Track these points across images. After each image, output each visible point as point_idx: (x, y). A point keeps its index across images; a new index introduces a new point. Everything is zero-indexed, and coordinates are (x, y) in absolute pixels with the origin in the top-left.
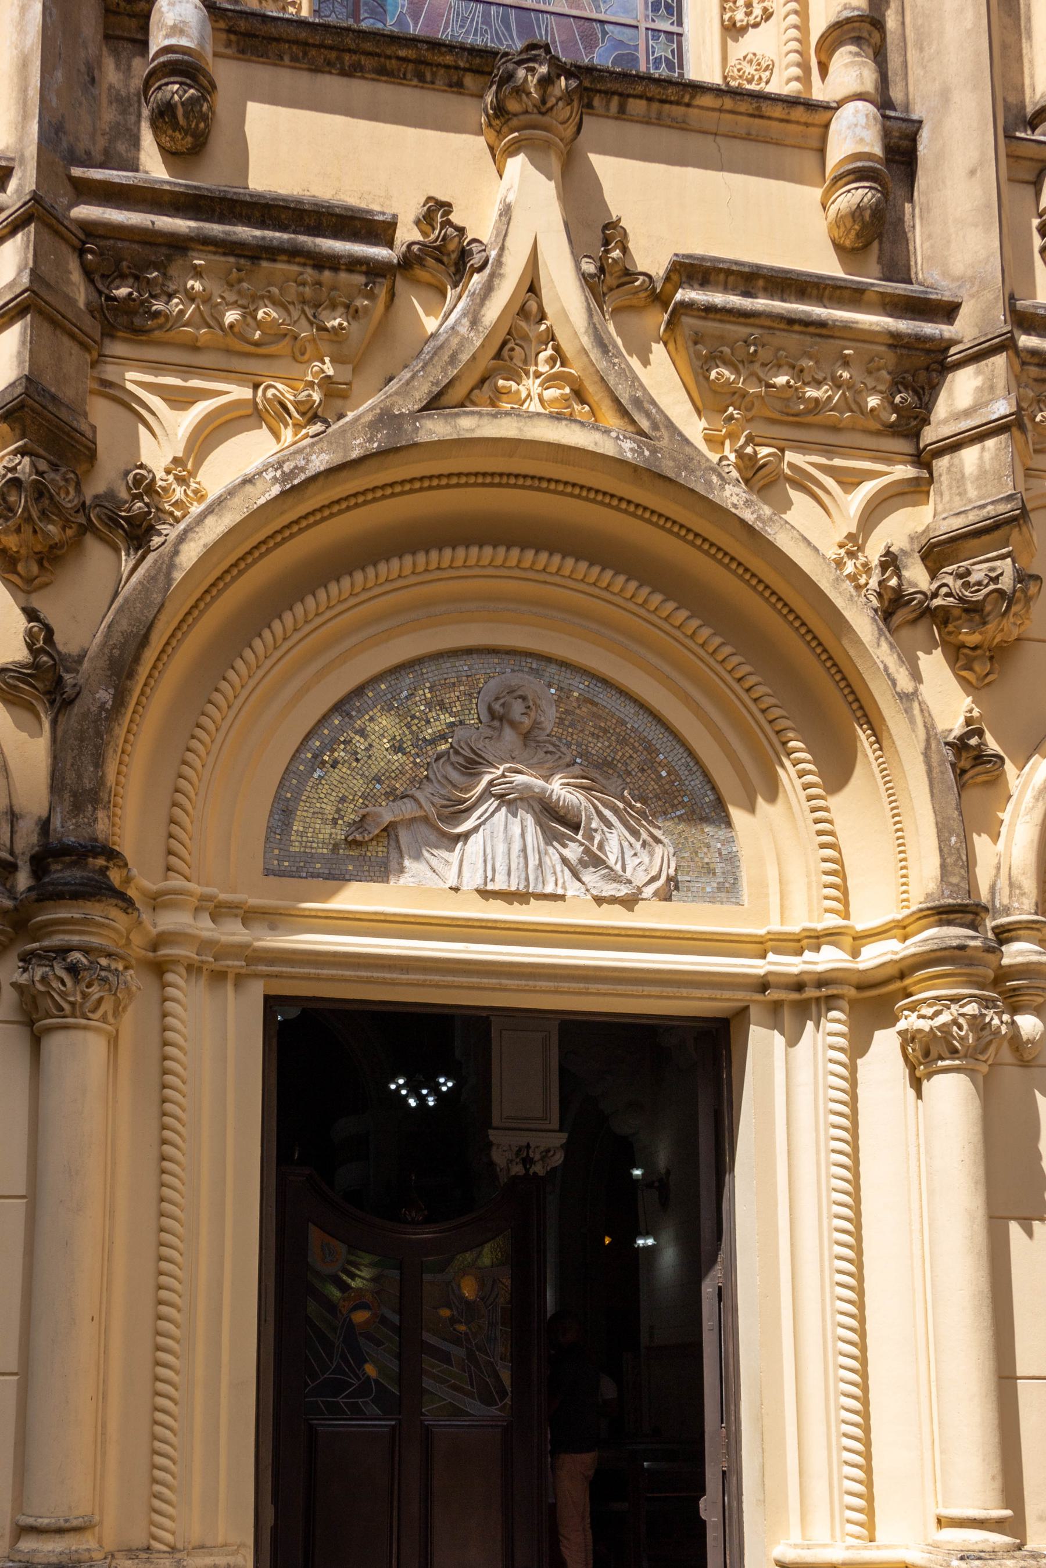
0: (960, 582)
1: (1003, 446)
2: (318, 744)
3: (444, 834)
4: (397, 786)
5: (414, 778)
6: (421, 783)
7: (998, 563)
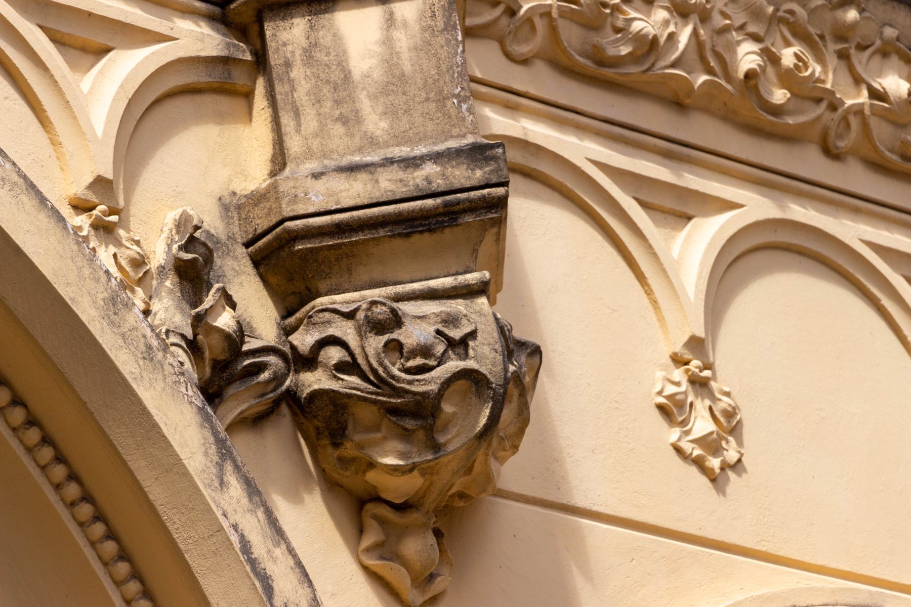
0: (376, 343)
1: (440, 24)
7: (458, 306)
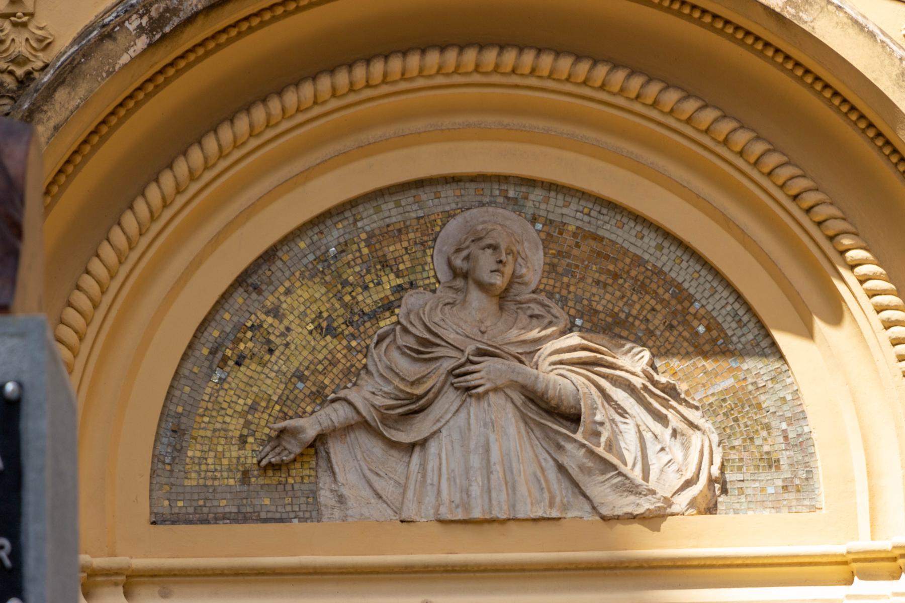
2: (216, 334)
3: (393, 445)
4: (327, 382)
5: (349, 369)
6: (358, 375)
